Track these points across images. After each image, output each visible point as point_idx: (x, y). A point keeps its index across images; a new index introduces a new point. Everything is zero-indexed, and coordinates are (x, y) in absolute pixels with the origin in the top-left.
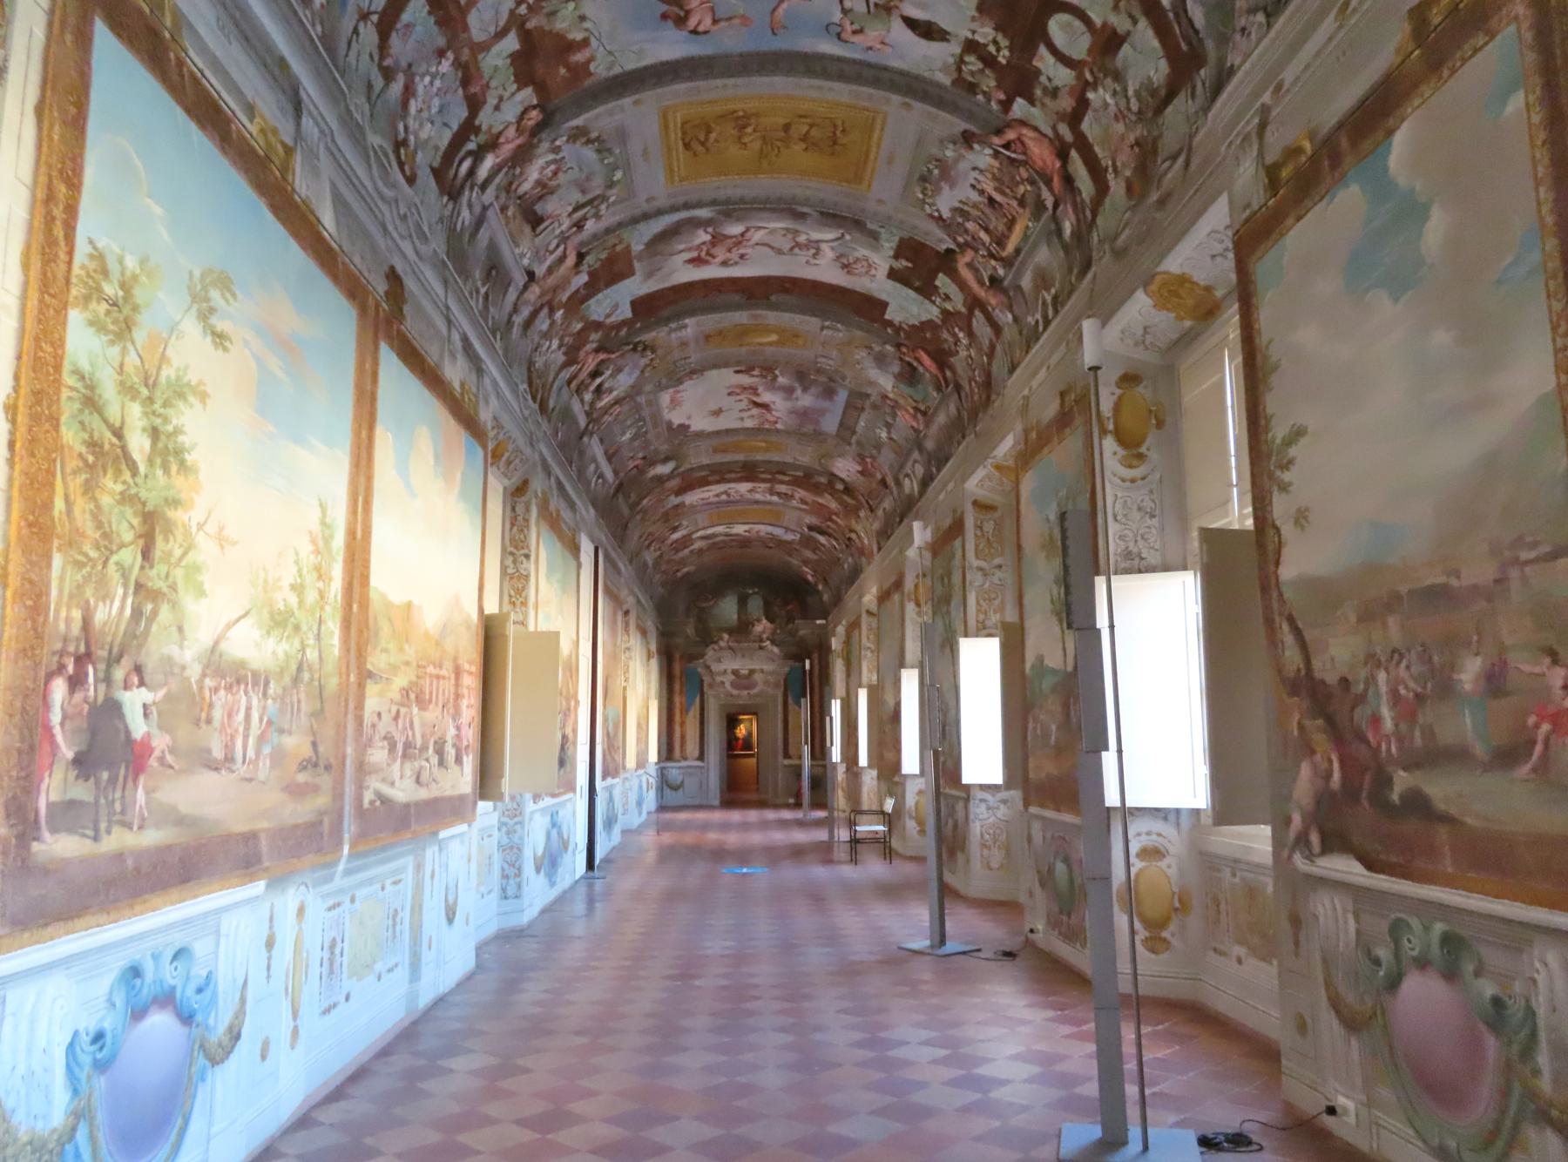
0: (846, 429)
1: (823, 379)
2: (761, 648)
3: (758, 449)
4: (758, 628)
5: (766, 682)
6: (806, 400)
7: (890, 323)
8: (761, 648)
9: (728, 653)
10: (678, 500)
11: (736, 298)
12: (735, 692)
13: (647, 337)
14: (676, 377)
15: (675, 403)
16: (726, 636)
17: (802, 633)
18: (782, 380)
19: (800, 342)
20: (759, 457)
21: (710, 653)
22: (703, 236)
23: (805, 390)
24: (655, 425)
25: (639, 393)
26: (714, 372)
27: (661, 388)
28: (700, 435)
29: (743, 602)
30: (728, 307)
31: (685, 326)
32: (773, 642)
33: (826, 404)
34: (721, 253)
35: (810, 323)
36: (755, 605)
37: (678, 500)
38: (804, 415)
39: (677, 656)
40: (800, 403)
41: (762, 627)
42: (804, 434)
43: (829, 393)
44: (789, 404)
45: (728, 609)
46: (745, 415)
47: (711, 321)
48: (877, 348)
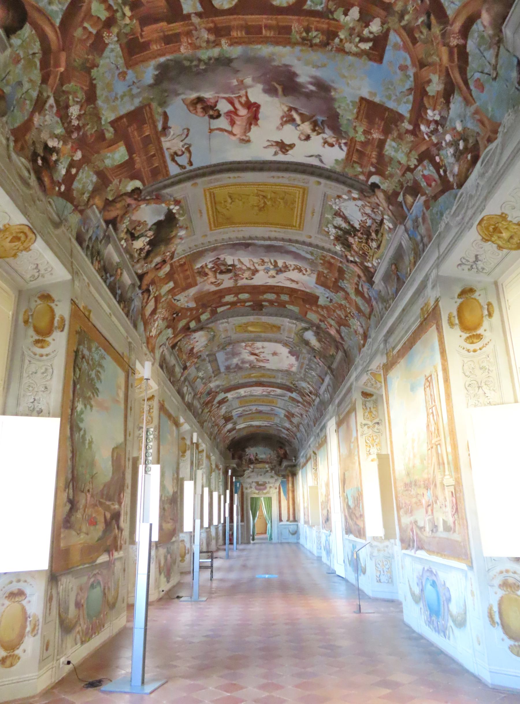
0: (214, 360)
1: (232, 371)
6: (235, 361)
10: (320, 291)
14: (287, 372)
15: (292, 366)
18: (248, 365)
20: (252, 318)
23: (237, 364)
24: (303, 363)
25: (301, 378)
27: (295, 374)
28: (285, 344)
33: (227, 364)
37: (320, 291)
38: (234, 354)
40: (237, 359)
42: (230, 344)
43: (228, 368)
44: (242, 356)
46: (262, 350)
47: (272, 380)
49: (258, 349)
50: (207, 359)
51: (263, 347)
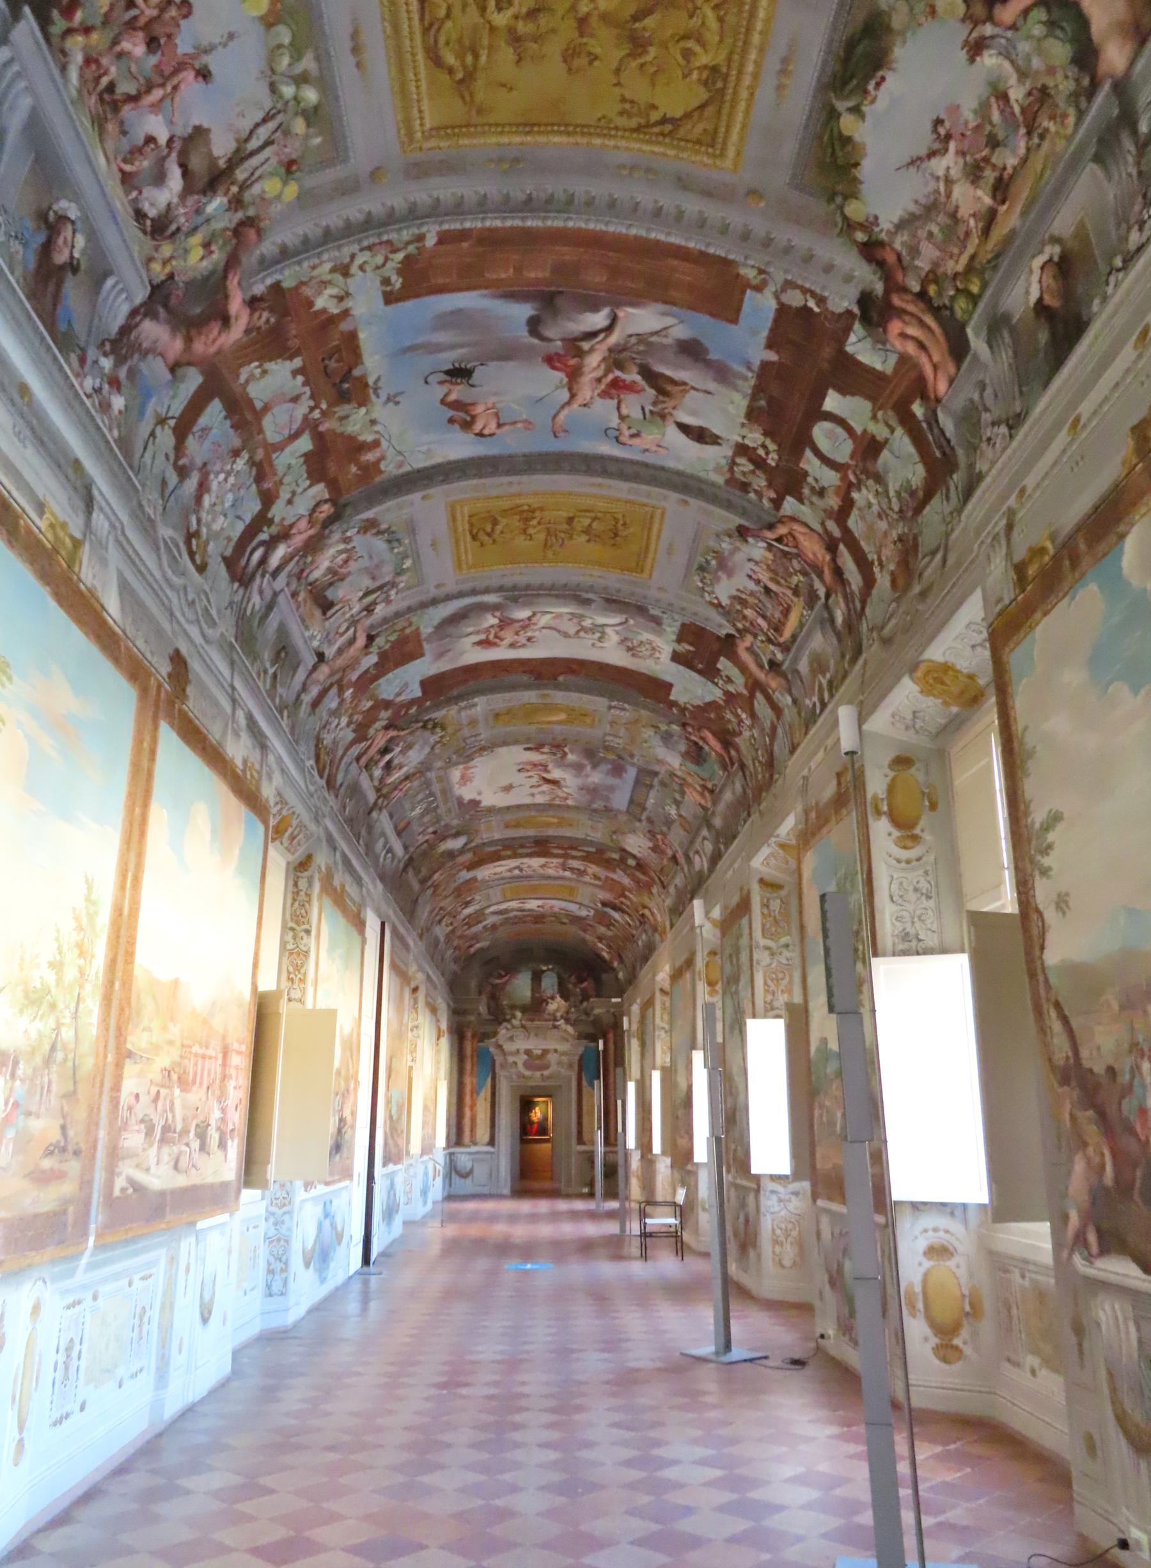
0: (636, 805)
1: (611, 757)
2: (555, 1027)
3: (549, 825)
4: (552, 1007)
5: (559, 1063)
6: (596, 777)
7: (674, 704)
8: (555, 1027)
9: (519, 1033)
11: (525, 678)
12: (528, 1073)
13: (438, 715)
14: (466, 754)
15: (465, 779)
16: (519, 1014)
17: (597, 1011)
18: (571, 757)
19: (588, 720)
20: (551, 832)
21: (503, 1032)
22: (491, 620)
23: (595, 766)
24: (446, 801)
25: (429, 769)
26: (504, 749)
27: (450, 764)
28: (491, 810)
29: (537, 977)
30: (513, 688)
31: (475, 705)
32: (567, 1021)
34: (508, 636)
35: (599, 703)
36: (549, 982)
38: (593, 791)
39: (469, 1034)
40: (590, 780)
41: (557, 1005)
42: (595, 811)
43: (618, 770)
44: (579, 781)
45: (521, 986)
46: (535, 791)
47: (501, 701)
48: (664, 727)
49: (543, 792)
50: (643, 817)
51: (533, 795)
